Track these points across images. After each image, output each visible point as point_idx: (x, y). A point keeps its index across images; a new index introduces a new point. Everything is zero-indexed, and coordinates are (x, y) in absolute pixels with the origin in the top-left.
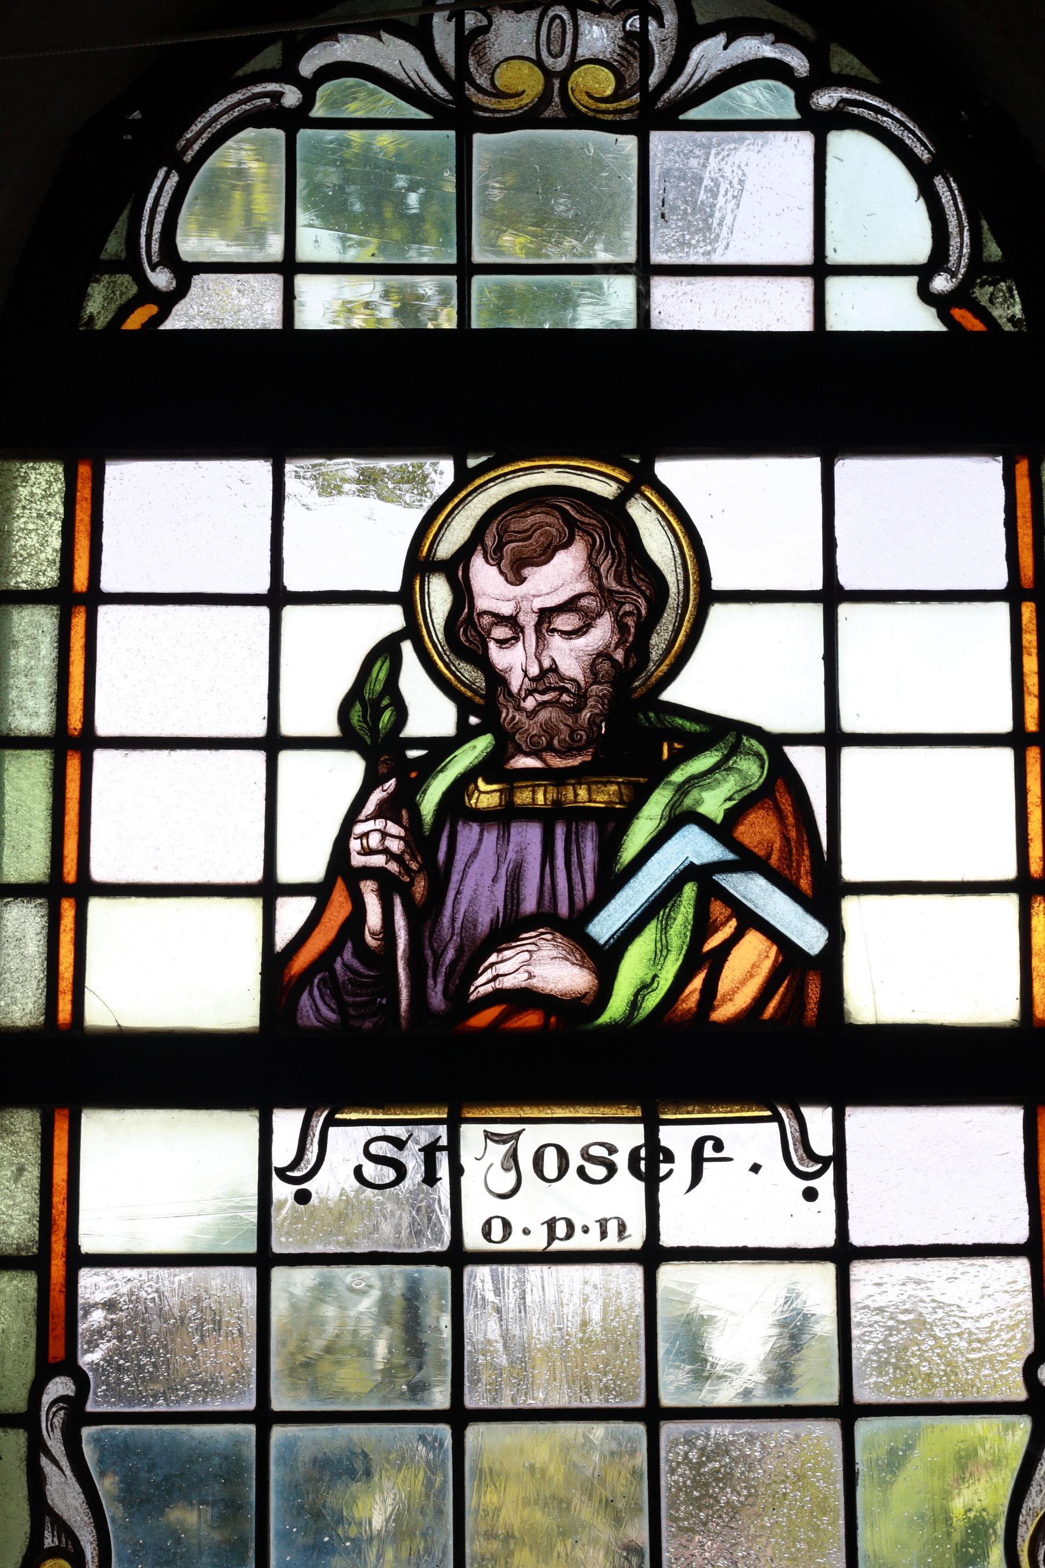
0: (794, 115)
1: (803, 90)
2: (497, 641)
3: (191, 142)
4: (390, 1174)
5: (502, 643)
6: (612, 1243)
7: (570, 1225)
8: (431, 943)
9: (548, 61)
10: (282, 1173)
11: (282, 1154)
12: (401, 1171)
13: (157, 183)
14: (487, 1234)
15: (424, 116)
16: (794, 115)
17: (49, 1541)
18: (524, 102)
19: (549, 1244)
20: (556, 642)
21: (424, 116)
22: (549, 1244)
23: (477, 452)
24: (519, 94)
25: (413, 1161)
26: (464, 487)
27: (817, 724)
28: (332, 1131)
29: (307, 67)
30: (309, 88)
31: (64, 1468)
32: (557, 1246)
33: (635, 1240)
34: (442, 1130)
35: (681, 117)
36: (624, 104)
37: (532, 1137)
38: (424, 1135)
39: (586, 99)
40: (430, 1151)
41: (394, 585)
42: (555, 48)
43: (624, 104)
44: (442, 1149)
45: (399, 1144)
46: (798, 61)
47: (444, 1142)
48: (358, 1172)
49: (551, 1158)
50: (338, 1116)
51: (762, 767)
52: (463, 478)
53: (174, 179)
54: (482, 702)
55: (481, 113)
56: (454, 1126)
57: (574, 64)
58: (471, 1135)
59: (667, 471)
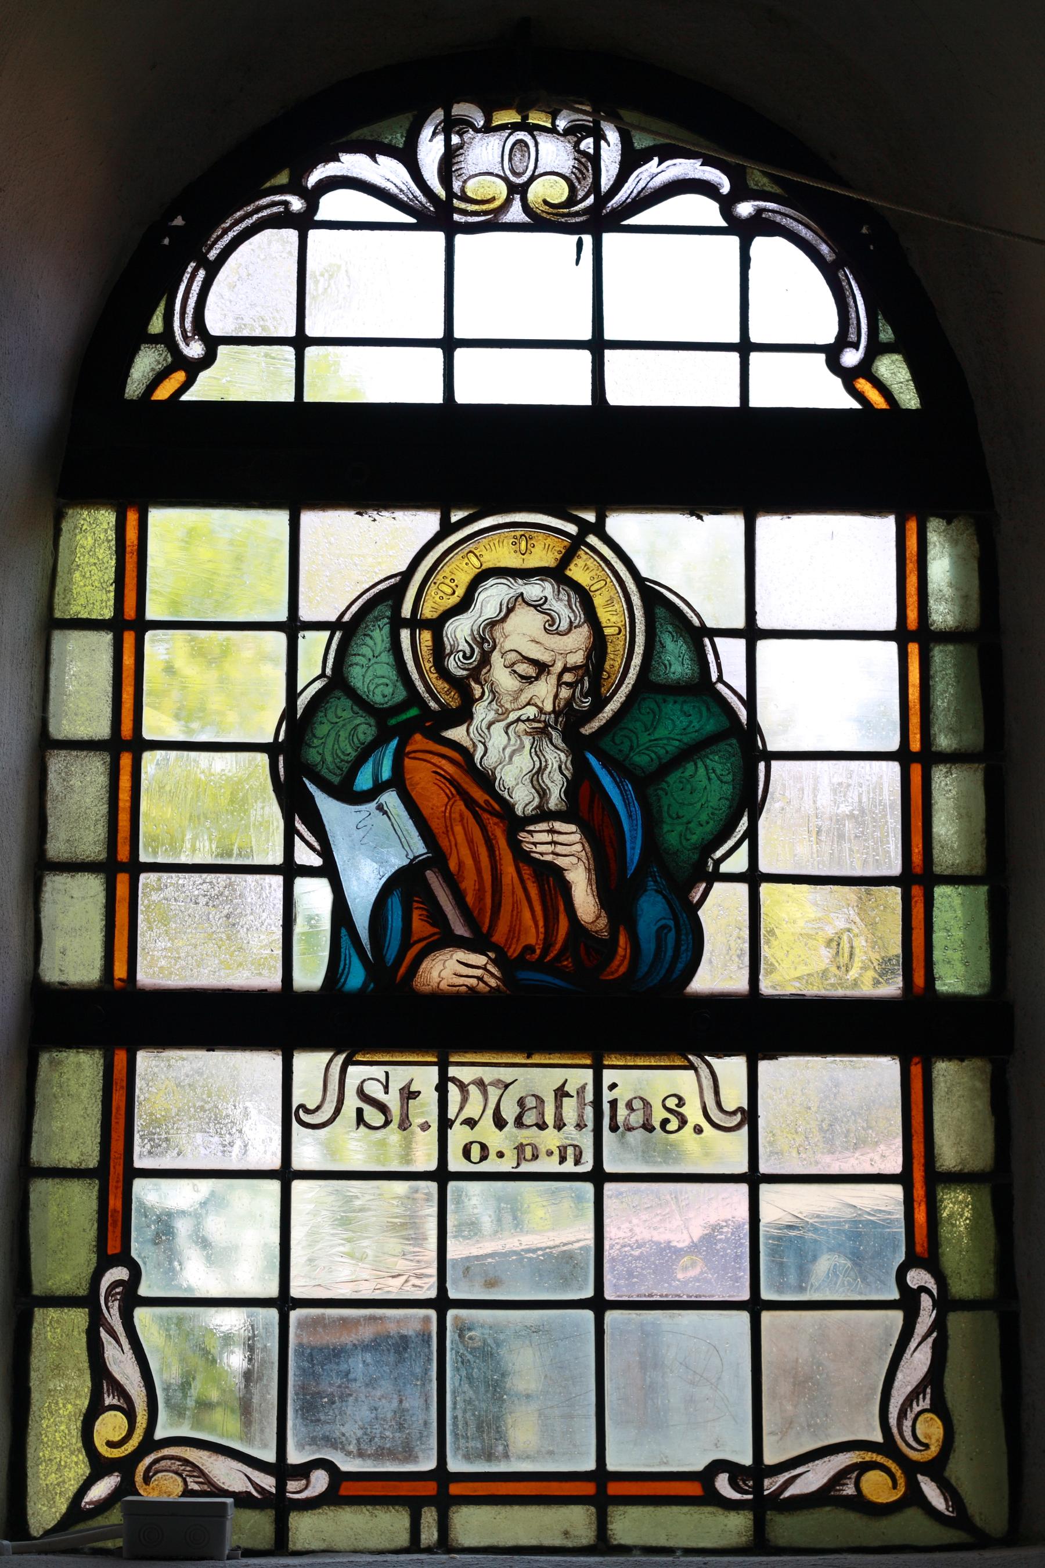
0: (723, 223)
14: (467, 1153)
16: (723, 223)
23: (460, 508)
52: (447, 529)
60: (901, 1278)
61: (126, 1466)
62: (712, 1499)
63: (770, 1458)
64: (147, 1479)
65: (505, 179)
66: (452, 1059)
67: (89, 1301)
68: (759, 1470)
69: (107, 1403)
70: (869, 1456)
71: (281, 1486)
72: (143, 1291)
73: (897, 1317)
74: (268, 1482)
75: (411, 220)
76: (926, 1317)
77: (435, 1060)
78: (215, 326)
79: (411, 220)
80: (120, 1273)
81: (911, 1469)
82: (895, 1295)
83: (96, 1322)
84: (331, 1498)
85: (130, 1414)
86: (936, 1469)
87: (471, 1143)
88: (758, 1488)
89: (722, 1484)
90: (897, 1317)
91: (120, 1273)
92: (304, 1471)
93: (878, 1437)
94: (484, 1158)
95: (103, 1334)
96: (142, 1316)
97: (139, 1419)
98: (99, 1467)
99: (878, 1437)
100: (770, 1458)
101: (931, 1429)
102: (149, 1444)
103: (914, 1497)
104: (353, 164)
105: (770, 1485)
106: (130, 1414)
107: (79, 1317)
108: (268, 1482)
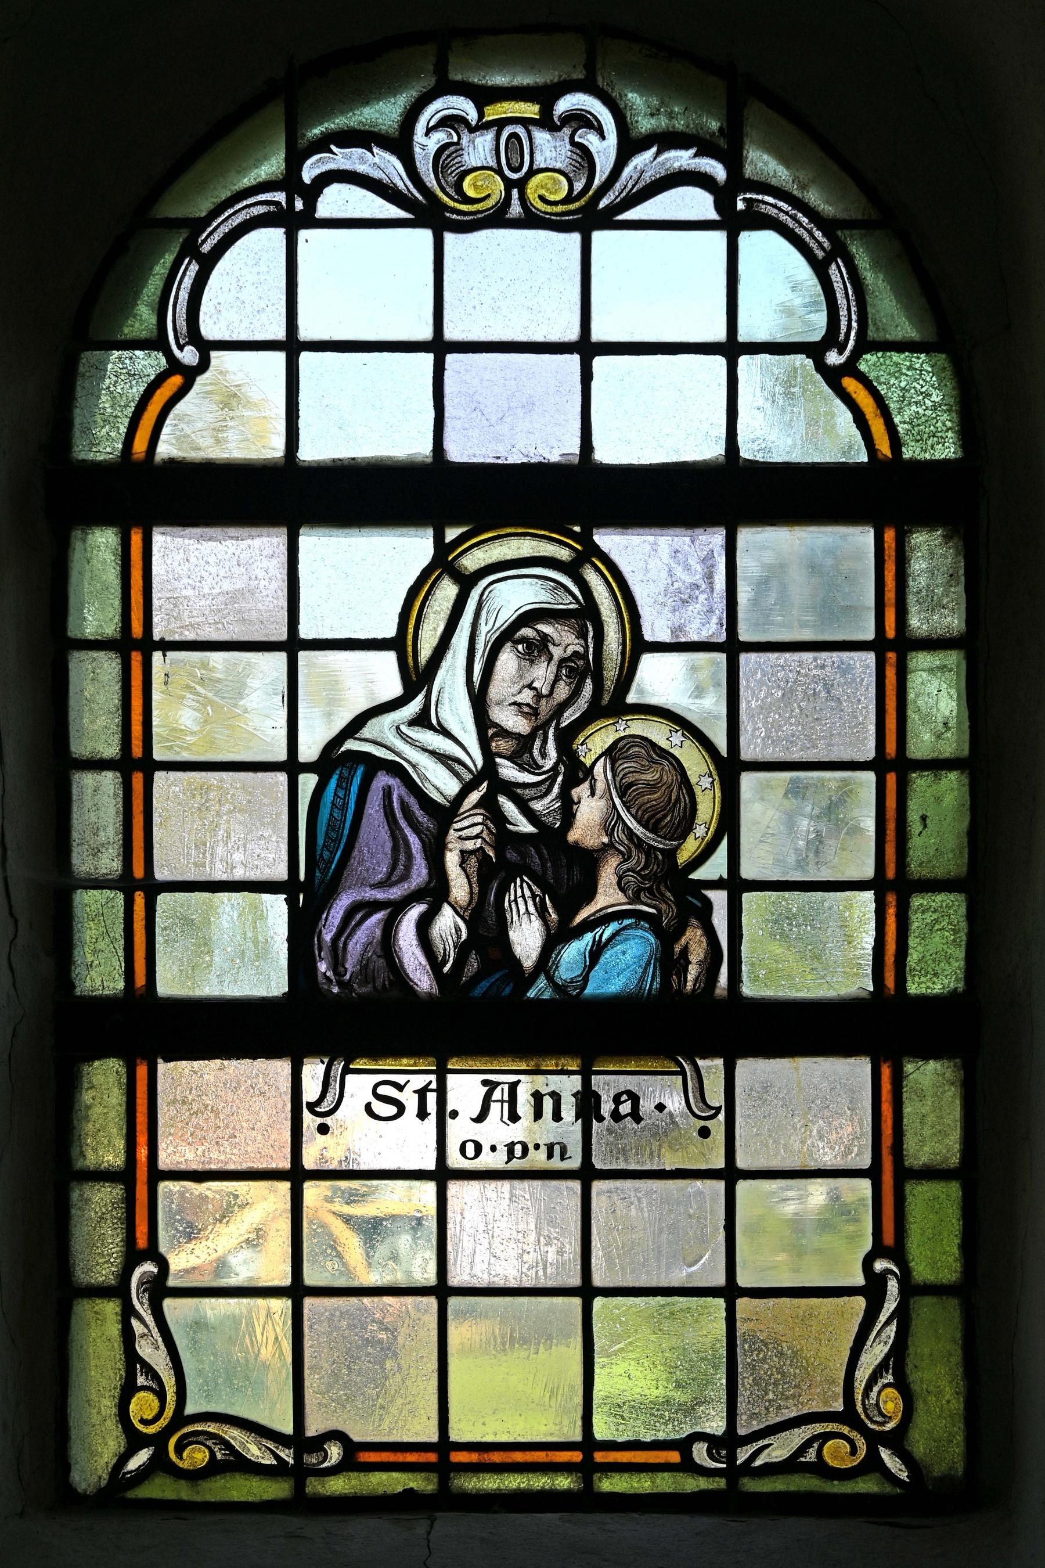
1: (723, 197)
4: (392, 1110)
6: (556, 1164)
12: (401, 1109)
17: (141, 1380)
29: (309, 173)
32: (516, 1164)
33: (574, 1162)
36: (572, 207)
39: (539, 205)
40: (422, 1093)
43: (572, 207)
46: (718, 171)
48: (368, 1108)
50: (351, 1066)
57: (532, 172)
59: (607, 540)
60: (867, 1263)
61: (159, 1441)
62: (689, 1466)
64: (180, 1449)
65: (499, 172)
66: (450, 1067)
67: (119, 1290)
69: (139, 1384)
71: (298, 1457)
72: (171, 1282)
73: (860, 1303)
74: (287, 1455)
75: (402, 214)
77: (434, 1068)
78: (210, 330)
79: (402, 214)
80: (149, 1267)
82: (860, 1280)
83: (128, 1312)
85: (161, 1394)
88: (732, 1458)
89: (700, 1452)
91: (149, 1267)
96: (168, 1304)
97: (169, 1398)
98: (134, 1441)
101: (891, 1403)
102: (180, 1419)
103: (872, 1464)
104: (343, 158)
105: (743, 1455)
106: (161, 1394)
107: (111, 1308)
108: (287, 1455)
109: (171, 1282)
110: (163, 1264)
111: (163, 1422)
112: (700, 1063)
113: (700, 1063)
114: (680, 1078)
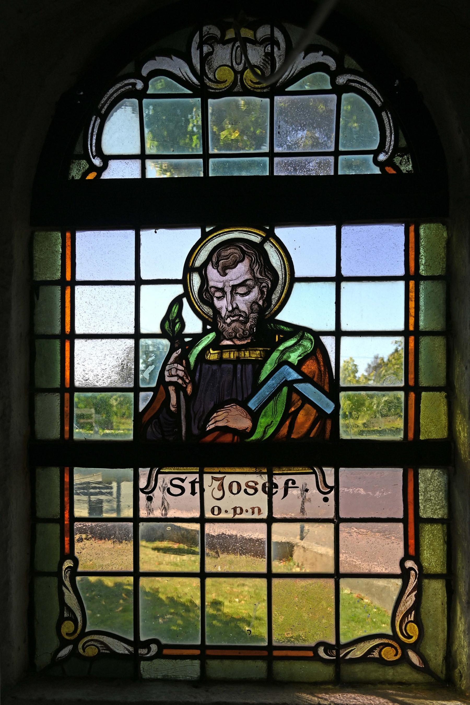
2: (217, 298)
3: (102, 107)
5: (218, 298)
7: (241, 509)
8: (193, 408)
9: (236, 66)
10: (142, 490)
11: (143, 483)
13: (92, 123)
15: (190, 92)
17: (66, 615)
18: (227, 85)
19: (234, 516)
20: (238, 297)
21: (190, 92)
22: (234, 516)
23: (210, 226)
24: (225, 82)
25: (187, 486)
26: (205, 239)
27: (332, 327)
28: (160, 476)
30: (146, 81)
31: (70, 590)
34: (197, 476)
35: (286, 90)
37: (228, 479)
38: (191, 478)
41: (180, 277)
42: (238, 61)
44: (197, 482)
45: (183, 481)
47: (198, 480)
49: (235, 486)
51: (312, 344)
53: (99, 121)
54: (211, 320)
55: (211, 90)
56: (201, 474)
58: (207, 478)
63: (343, 640)
68: (338, 646)
70: (386, 641)
72: (80, 569)
76: (413, 582)
81: (404, 647)
84: (159, 655)
86: (415, 647)
87: (214, 507)
90: (399, 582)
92: (147, 644)
93: (390, 633)
94: (219, 513)
95: (64, 588)
99: (390, 633)
100: (343, 640)
101: (413, 630)
109: (80, 569)
110: (76, 561)
111: (76, 635)
112: (324, 469)
113: (324, 469)
114: (314, 475)
